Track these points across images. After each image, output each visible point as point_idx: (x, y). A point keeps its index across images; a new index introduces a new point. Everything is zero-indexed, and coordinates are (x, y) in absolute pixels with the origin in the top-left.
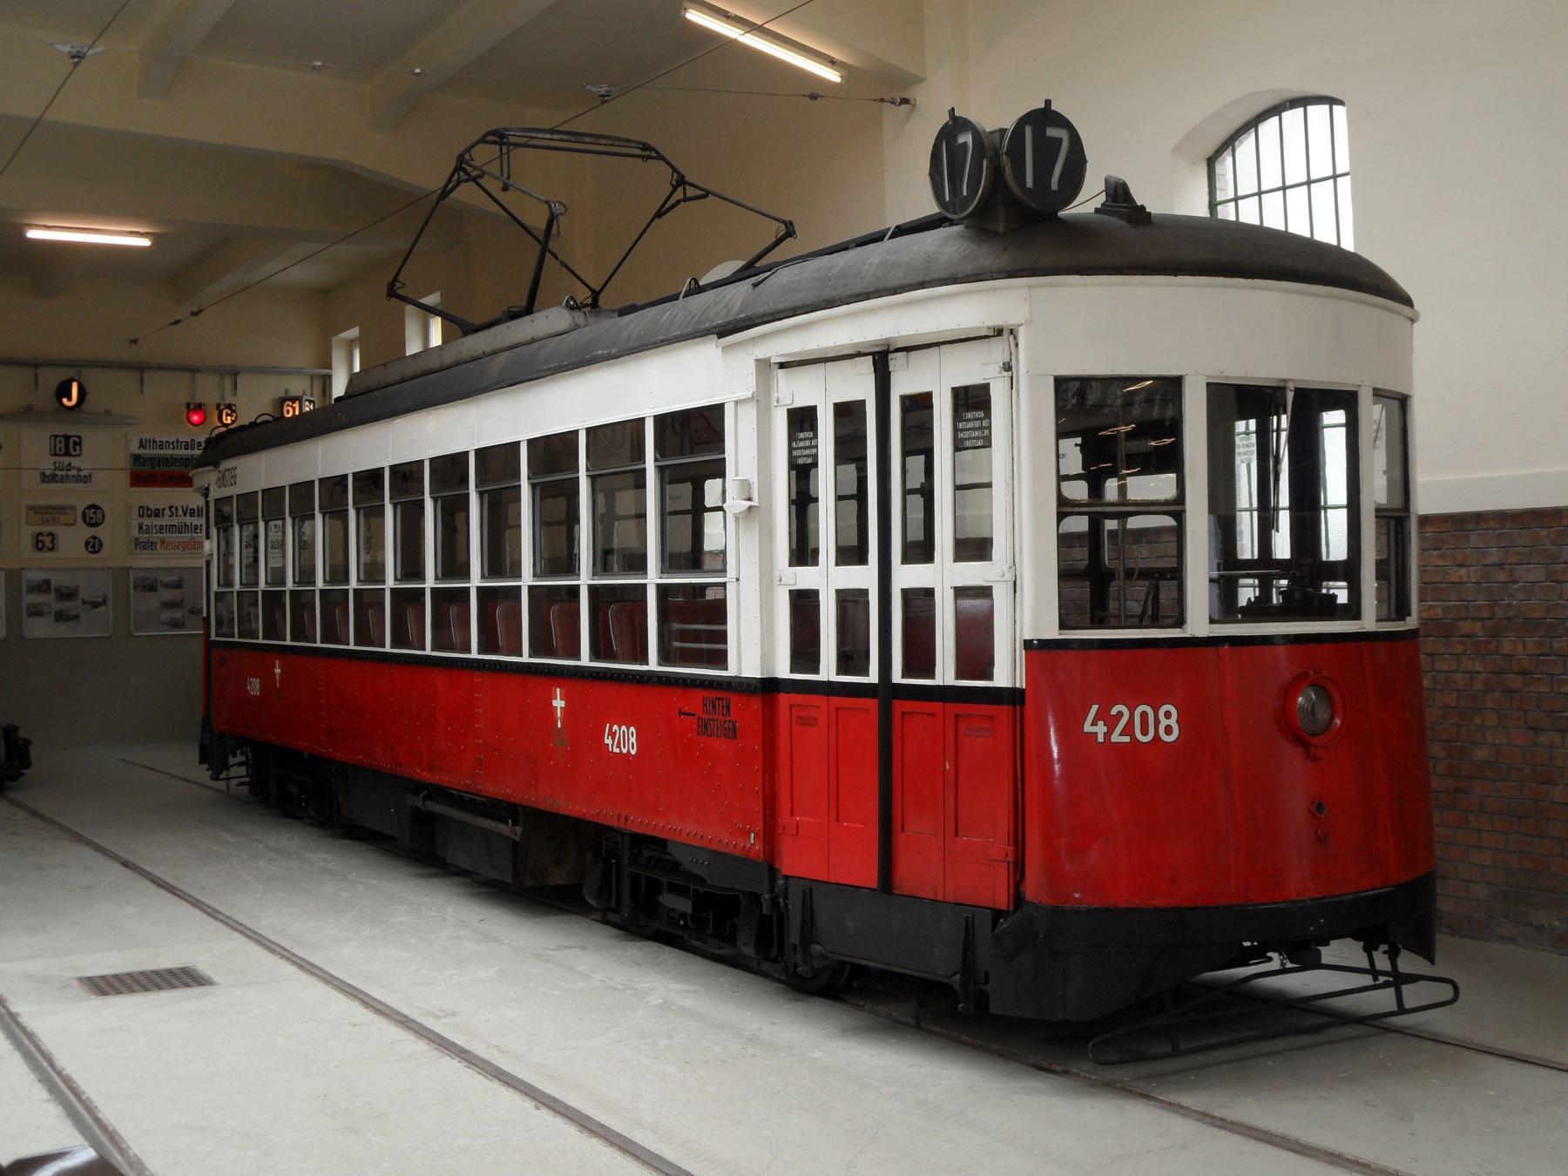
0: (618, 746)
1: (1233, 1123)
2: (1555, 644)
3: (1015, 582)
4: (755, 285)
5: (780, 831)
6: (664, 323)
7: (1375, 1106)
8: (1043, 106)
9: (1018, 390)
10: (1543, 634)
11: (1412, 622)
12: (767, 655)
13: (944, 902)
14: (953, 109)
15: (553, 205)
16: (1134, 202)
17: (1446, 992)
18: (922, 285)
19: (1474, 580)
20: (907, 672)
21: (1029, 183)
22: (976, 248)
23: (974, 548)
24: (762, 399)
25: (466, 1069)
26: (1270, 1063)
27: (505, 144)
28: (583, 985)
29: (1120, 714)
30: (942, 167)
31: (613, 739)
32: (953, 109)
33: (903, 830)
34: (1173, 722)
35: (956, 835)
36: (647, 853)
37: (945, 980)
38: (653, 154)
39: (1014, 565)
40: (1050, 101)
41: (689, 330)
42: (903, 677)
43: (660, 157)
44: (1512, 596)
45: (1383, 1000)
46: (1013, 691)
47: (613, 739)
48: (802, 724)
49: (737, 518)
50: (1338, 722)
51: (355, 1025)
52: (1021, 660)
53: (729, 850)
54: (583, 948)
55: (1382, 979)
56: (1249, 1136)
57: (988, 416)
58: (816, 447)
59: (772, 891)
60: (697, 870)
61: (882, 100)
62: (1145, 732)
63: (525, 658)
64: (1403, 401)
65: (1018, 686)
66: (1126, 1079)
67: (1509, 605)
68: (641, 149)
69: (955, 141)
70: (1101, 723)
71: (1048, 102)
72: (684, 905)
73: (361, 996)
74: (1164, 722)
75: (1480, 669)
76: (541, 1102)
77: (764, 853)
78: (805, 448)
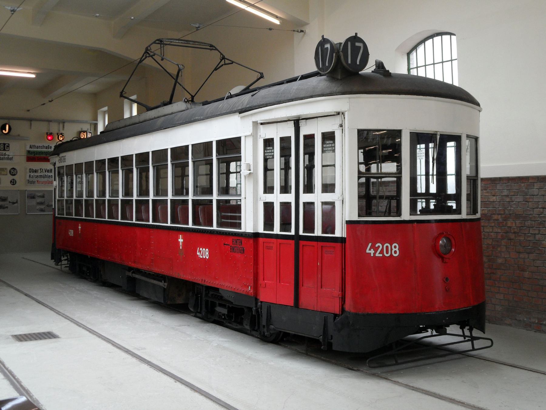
0: (202, 255)
1: (416, 388)
2: (526, 223)
3: (343, 200)
4: (252, 96)
5: (259, 286)
6: (220, 108)
7: (465, 382)
8: (354, 35)
9: (345, 134)
10: (522, 220)
11: (478, 216)
12: (255, 225)
13: (317, 311)
14: (323, 35)
15: (179, 66)
16: (385, 69)
17: (488, 343)
18: (312, 97)
19: (498, 201)
20: (305, 230)
21: (349, 62)
22: (331, 84)
23: (328, 188)
24: (254, 136)
25: (149, 368)
26: (428, 367)
27: (162, 44)
28: (189, 339)
29: (379, 246)
30: (319, 55)
31: (200, 253)
32: (323, 35)
33: (303, 286)
34: (397, 249)
35: (321, 288)
36: (211, 293)
37: (317, 338)
38: (214, 48)
39: (343, 194)
40: (357, 33)
41: (229, 111)
42: (303, 233)
43: (216, 49)
44: (511, 206)
45: (467, 346)
46: (342, 238)
47: (200, 253)
48: (267, 249)
49: (245, 177)
50: (453, 250)
51: (110, 352)
52: (345, 227)
53: (241, 292)
54: (189, 326)
55: (467, 339)
56: (422, 393)
57: (334, 142)
58: (274, 152)
59: (256, 306)
60: (230, 299)
61: (294, 31)
62: (387, 253)
63: (169, 224)
64: (476, 139)
65: (343, 236)
66: (379, 373)
67: (510, 210)
68: (210, 47)
69: (324, 47)
70: (372, 250)
71: (356, 34)
72: (224, 311)
73: (112, 342)
74: (394, 249)
75: (500, 231)
76: (177, 380)
77: (254, 293)
78: (270, 153)
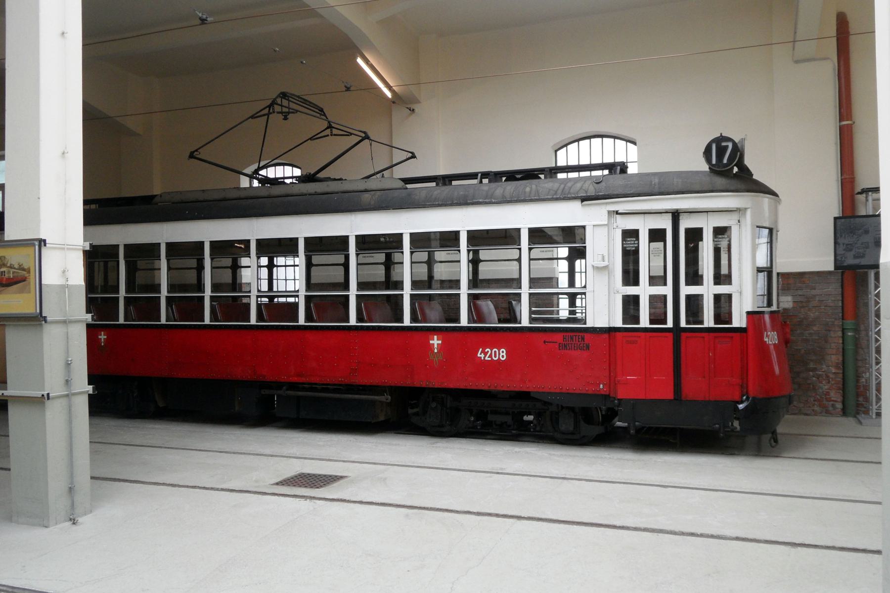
20: (688, 322)
23: (721, 278)
68: (319, 110)
71: (721, 134)
